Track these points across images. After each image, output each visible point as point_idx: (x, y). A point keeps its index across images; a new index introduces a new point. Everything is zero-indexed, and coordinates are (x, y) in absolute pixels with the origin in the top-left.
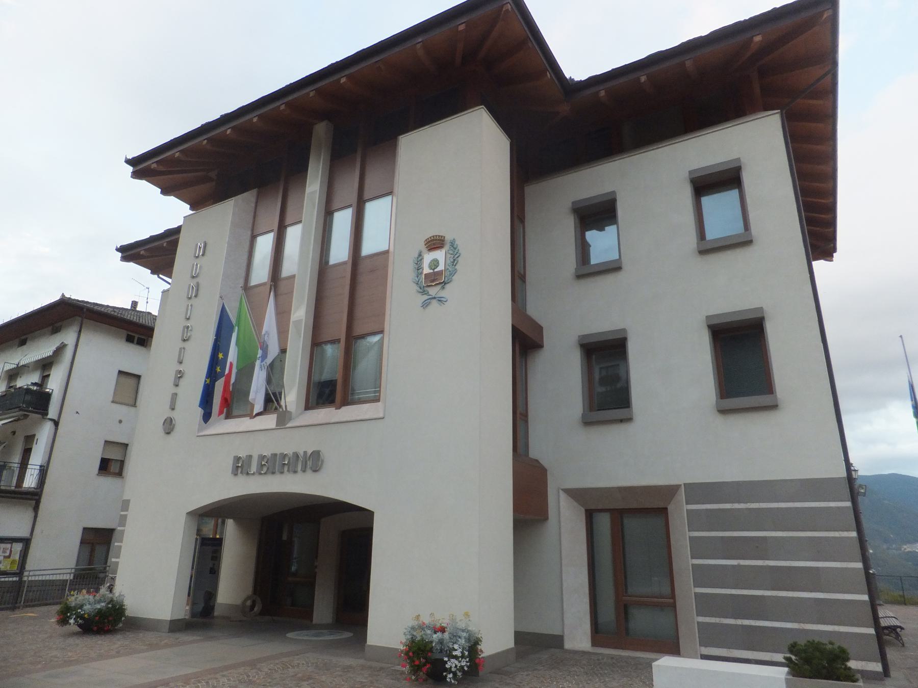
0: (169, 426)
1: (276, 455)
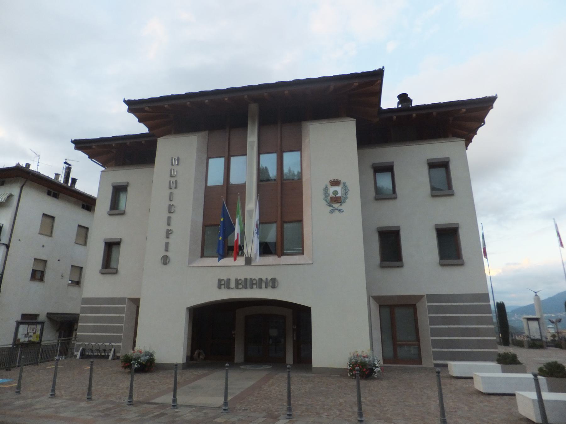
0: (165, 260)
1: (247, 279)
